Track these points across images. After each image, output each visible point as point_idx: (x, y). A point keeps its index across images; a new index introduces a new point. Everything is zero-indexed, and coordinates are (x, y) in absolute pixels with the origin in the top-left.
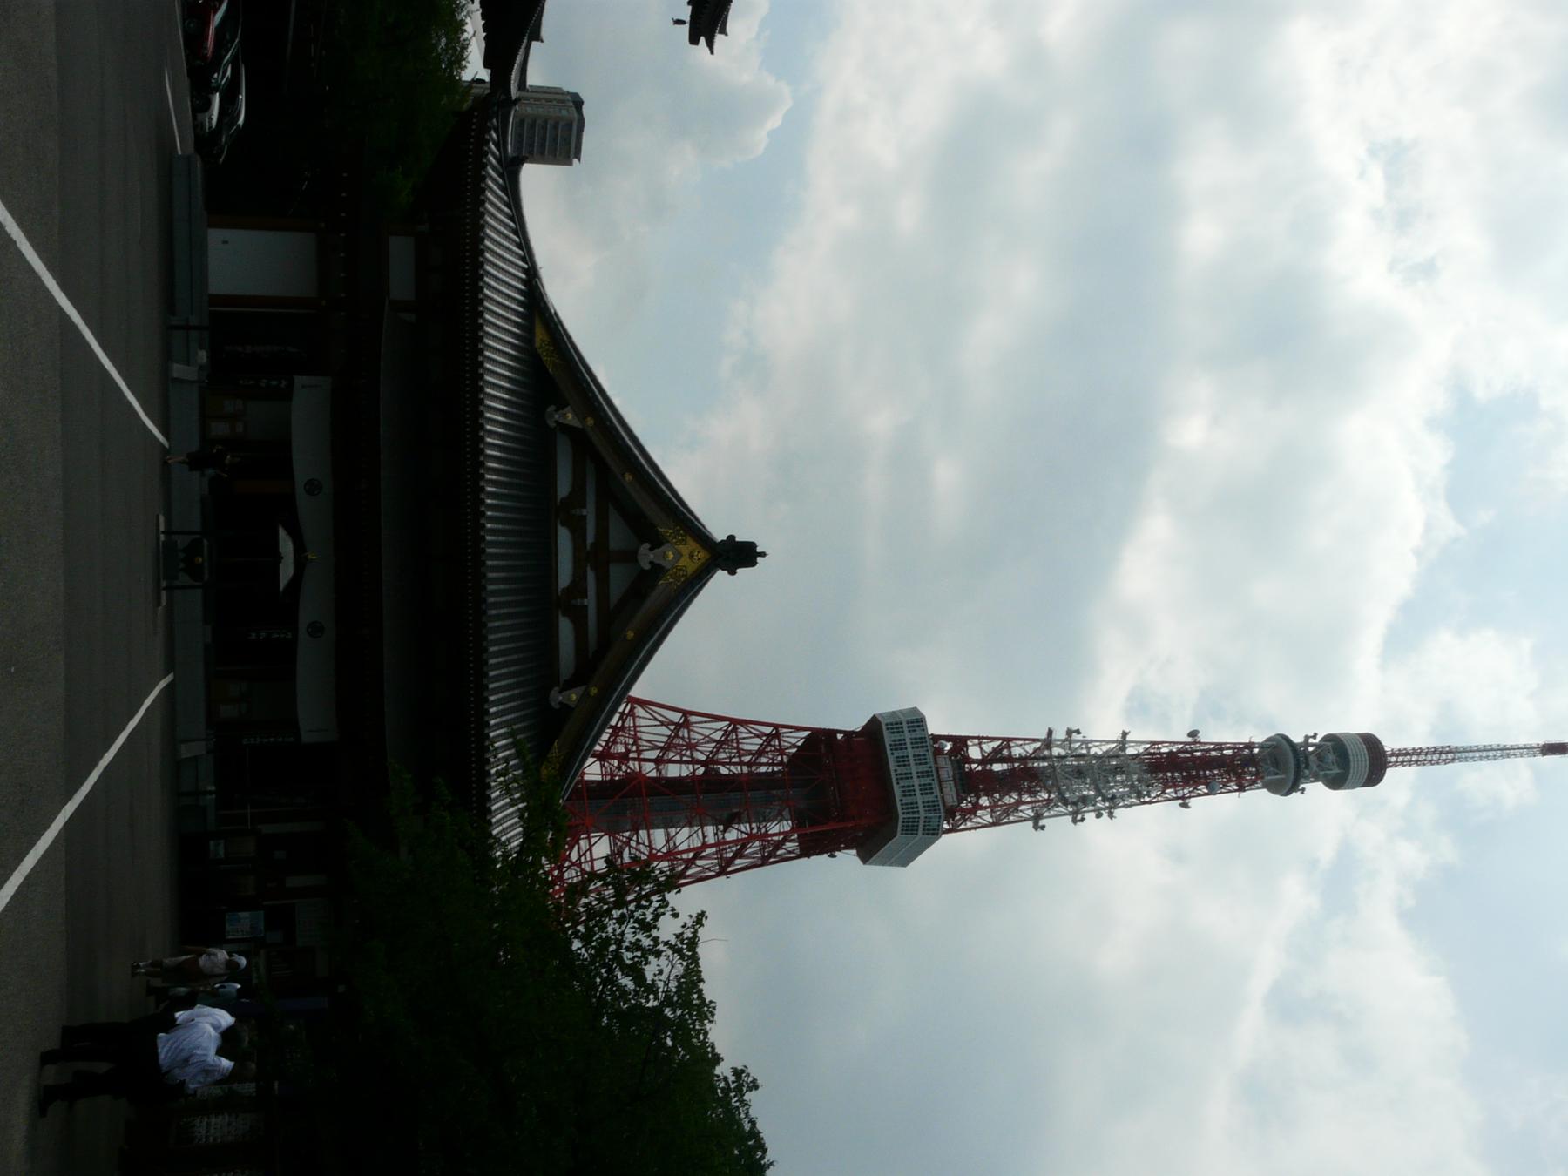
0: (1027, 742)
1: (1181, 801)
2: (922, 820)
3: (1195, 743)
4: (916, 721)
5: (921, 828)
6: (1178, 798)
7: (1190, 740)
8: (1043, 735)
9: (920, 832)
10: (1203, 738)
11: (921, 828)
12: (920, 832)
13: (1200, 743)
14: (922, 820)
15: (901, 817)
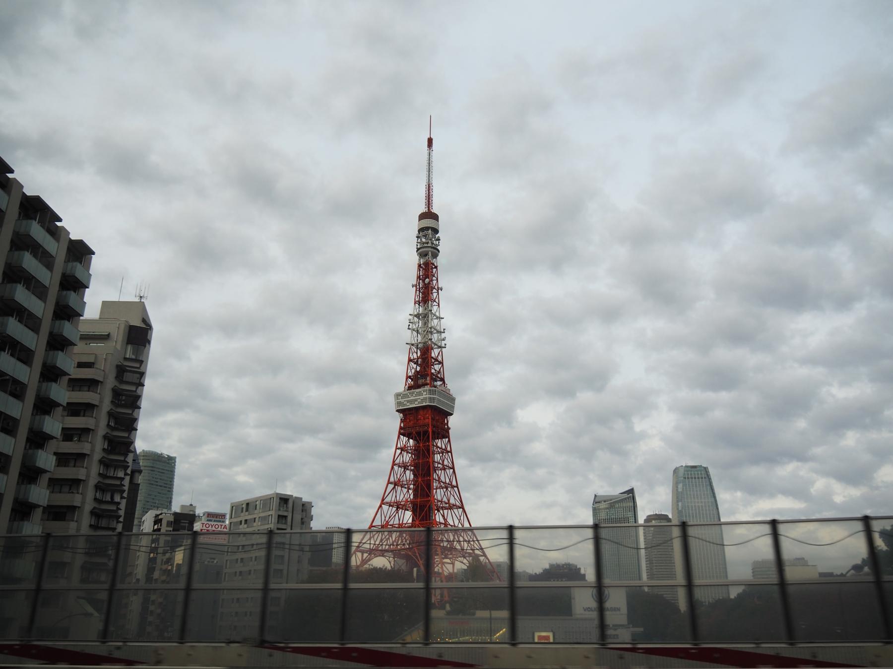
0: (411, 352)
1: (440, 291)
2: (430, 396)
3: (416, 287)
4: (398, 395)
5: (433, 396)
6: (438, 292)
7: (415, 288)
8: (408, 346)
9: (435, 396)
10: (415, 283)
11: (433, 396)
12: (435, 396)
13: (416, 285)
14: (430, 396)
15: (428, 404)
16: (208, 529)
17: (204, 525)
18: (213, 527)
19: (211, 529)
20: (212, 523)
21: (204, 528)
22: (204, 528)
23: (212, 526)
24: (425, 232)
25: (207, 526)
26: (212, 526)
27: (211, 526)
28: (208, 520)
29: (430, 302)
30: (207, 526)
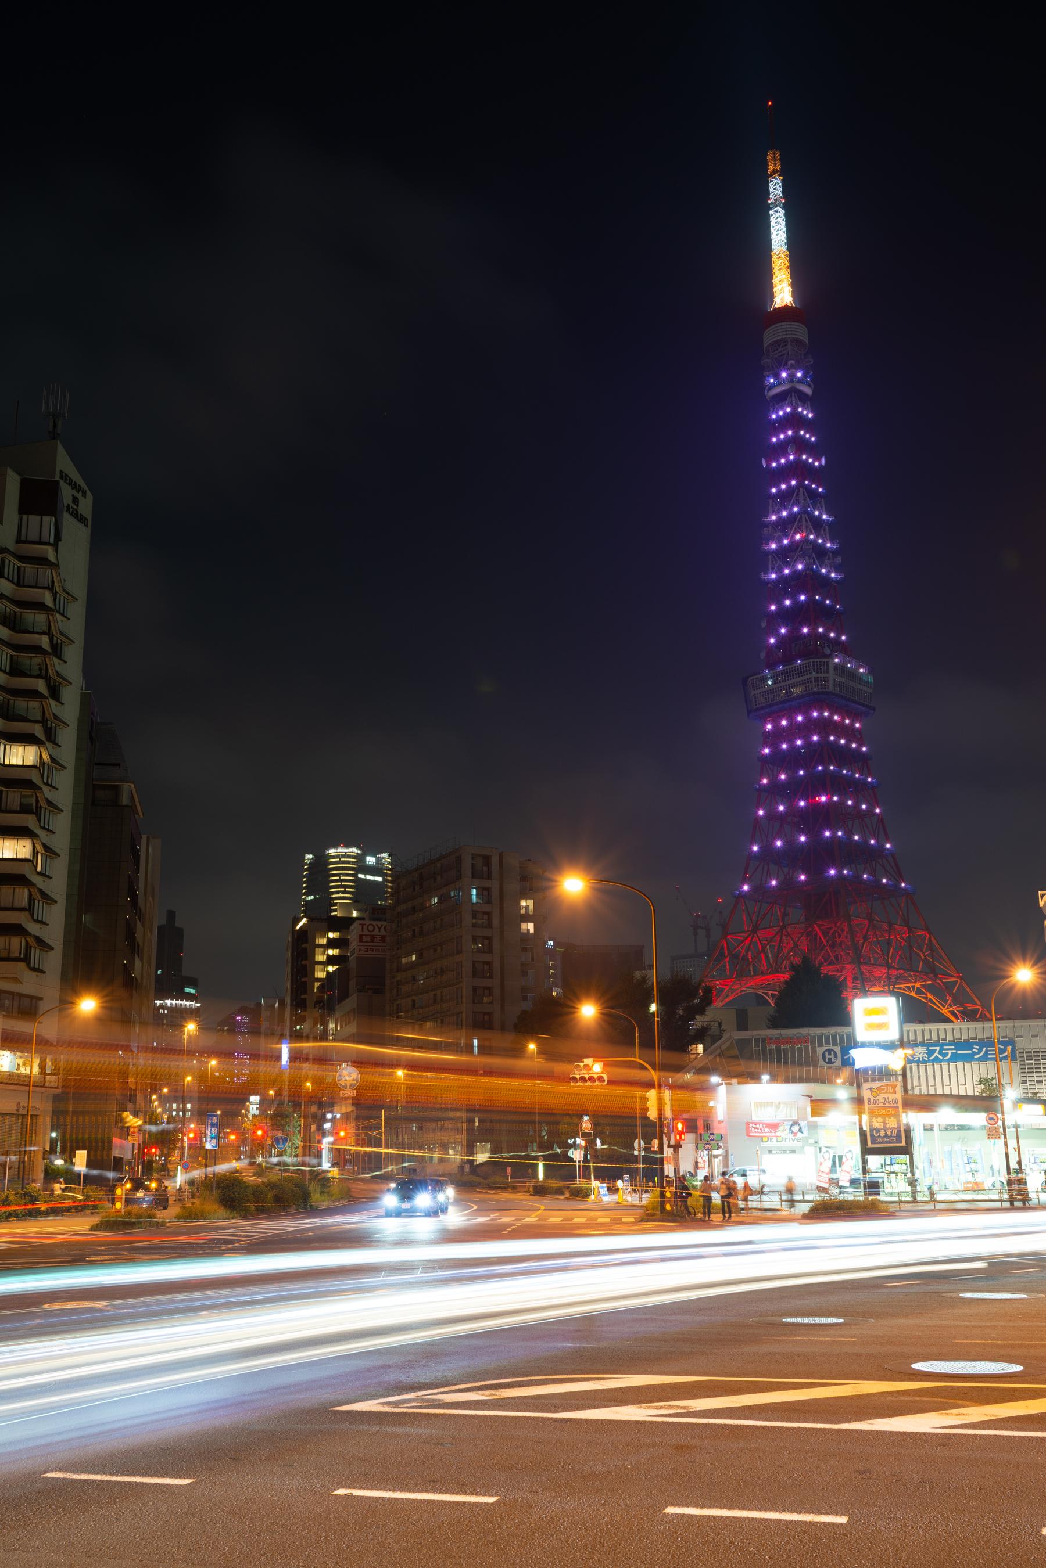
5: (823, 675)
16: (372, 934)
17: (365, 927)
18: (382, 930)
19: (379, 934)
20: (380, 923)
21: (366, 932)
22: (366, 932)
23: (379, 929)
24: (779, 350)
25: (371, 928)
26: (379, 929)
27: (377, 929)
28: (374, 920)
29: (801, 489)
30: (371, 928)
